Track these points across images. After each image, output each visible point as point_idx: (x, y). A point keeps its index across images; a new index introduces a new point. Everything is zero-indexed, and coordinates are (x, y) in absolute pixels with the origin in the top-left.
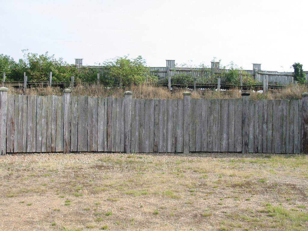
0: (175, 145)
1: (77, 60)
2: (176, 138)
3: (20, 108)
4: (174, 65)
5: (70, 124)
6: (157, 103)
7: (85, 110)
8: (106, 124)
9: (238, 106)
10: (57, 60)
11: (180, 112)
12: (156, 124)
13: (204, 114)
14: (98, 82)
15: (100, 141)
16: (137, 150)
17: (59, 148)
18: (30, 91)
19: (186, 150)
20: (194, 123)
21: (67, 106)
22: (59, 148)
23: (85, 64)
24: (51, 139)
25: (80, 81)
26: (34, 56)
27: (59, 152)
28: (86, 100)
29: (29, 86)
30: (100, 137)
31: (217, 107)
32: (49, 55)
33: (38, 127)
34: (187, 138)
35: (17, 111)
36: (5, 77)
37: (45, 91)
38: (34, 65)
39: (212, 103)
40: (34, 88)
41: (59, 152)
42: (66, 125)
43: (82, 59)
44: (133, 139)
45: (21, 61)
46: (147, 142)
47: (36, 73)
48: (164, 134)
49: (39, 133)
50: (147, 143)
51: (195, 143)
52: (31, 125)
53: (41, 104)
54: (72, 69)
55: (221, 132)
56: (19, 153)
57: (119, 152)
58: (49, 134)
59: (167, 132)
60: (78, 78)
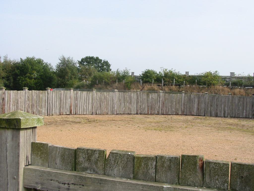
0: (224, 114)
1: (186, 72)
2: (225, 112)
3: (166, 98)
4: (234, 75)
5: (184, 104)
6: (218, 97)
7: (190, 100)
8: (197, 105)
9: (251, 99)
10: (177, 72)
11: (227, 101)
12: (217, 105)
13: (236, 102)
14: (196, 84)
15: (195, 111)
16: (209, 115)
17: (180, 113)
18: (165, 88)
19: (229, 116)
20: (232, 105)
21: (183, 98)
22: (180, 113)
23: (190, 74)
24: (177, 109)
25: (188, 83)
26: (166, 70)
27: (180, 115)
28: (190, 96)
29: (164, 85)
30: (195, 110)
31: (242, 99)
32: (173, 70)
33: (173, 105)
34: (229, 111)
35: (165, 99)
36: (153, 81)
37: (172, 88)
38: (166, 75)
39: (240, 98)
40: (166, 86)
41: (180, 115)
42: (183, 105)
43: (188, 72)
44: (208, 111)
45: (160, 72)
46: (213, 112)
47: (167, 79)
48: (220, 110)
49: (173, 108)
50: (213, 113)
51: (232, 113)
52: (170, 104)
53: (174, 97)
54: (184, 77)
55: (243, 110)
56: (166, 114)
57: (202, 116)
58: (176, 108)
59: (221, 109)
60: (187, 82)
